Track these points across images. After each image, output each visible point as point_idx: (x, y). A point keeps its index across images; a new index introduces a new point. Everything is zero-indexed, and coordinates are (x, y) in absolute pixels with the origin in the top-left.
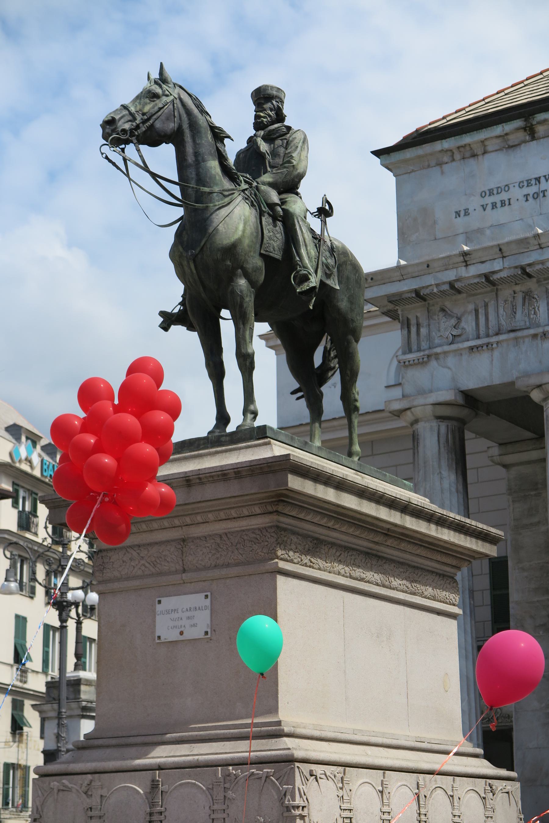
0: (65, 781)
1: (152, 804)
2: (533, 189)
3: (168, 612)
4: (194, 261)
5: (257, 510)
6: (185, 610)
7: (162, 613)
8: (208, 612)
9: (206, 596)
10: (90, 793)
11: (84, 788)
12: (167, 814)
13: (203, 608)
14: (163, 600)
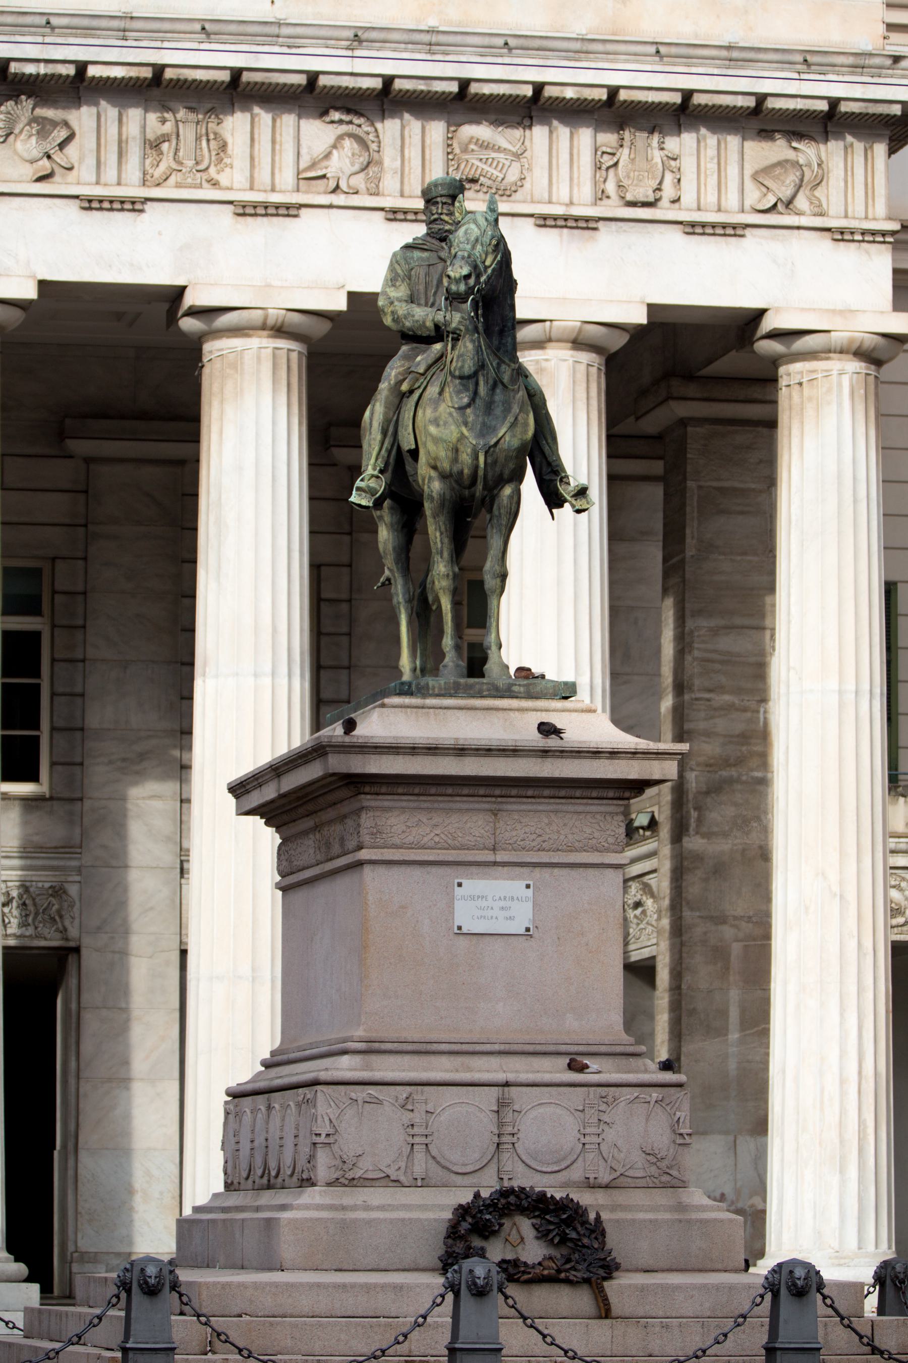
0: (372, 1090)
1: (501, 1124)
3: (472, 898)
4: (486, 453)
7: (463, 898)
8: (530, 905)
9: (528, 886)
10: (411, 1108)
11: (401, 1101)
12: (520, 1135)
13: (524, 899)
14: (464, 882)
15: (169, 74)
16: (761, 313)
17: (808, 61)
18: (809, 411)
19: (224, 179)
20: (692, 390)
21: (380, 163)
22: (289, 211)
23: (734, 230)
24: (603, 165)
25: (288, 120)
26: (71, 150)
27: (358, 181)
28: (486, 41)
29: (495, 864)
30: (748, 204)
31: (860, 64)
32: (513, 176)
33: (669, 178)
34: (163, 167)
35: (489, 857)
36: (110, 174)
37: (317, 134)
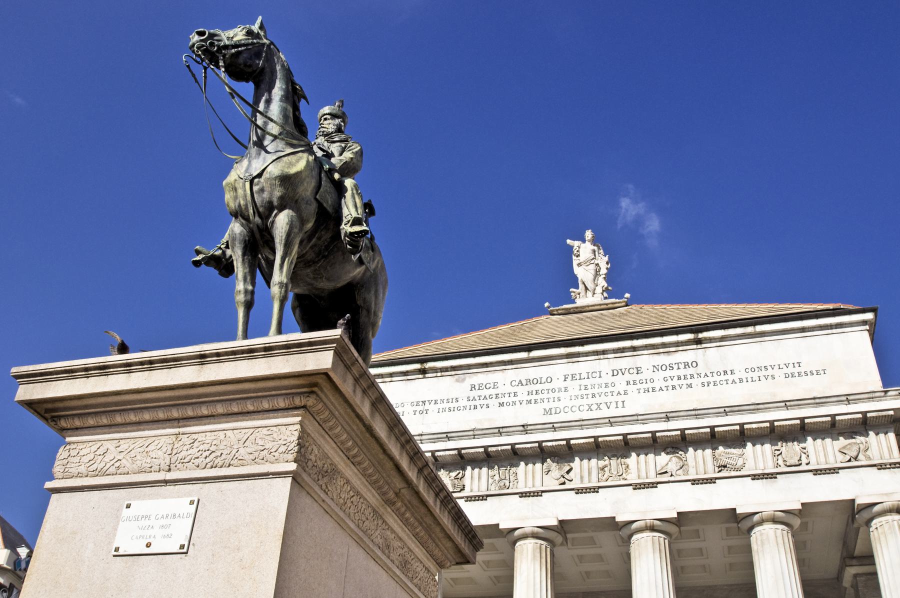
2: (421, 408)
5: (281, 403)
6: (160, 516)
7: (128, 519)
9: (192, 503)
15: (600, 439)
16: (853, 501)
17: (848, 399)
18: (883, 538)
19: (628, 477)
20: (854, 562)
21: (687, 465)
22: (653, 485)
23: (834, 471)
24: (778, 454)
25: (651, 456)
26: (571, 473)
27: (680, 472)
28: (717, 410)
29: (166, 482)
30: (838, 461)
31: (871, 396)
32: (740, 462)
33: (803, 456)
34: (606, 476)
35: (161, 476)
36: (586, 479)
37: (663, 458)
